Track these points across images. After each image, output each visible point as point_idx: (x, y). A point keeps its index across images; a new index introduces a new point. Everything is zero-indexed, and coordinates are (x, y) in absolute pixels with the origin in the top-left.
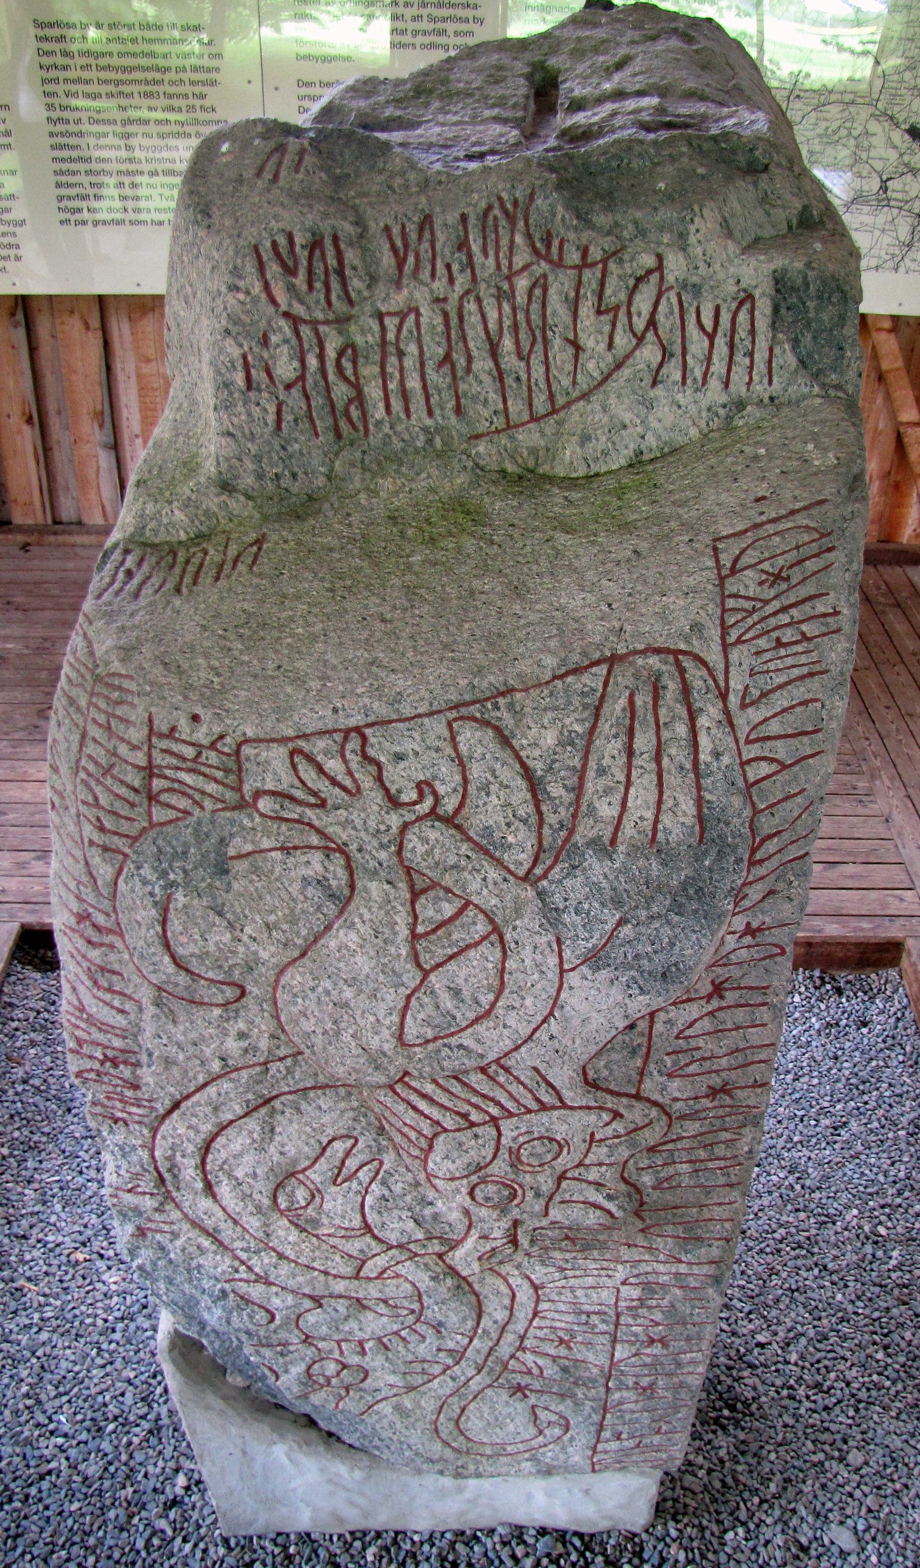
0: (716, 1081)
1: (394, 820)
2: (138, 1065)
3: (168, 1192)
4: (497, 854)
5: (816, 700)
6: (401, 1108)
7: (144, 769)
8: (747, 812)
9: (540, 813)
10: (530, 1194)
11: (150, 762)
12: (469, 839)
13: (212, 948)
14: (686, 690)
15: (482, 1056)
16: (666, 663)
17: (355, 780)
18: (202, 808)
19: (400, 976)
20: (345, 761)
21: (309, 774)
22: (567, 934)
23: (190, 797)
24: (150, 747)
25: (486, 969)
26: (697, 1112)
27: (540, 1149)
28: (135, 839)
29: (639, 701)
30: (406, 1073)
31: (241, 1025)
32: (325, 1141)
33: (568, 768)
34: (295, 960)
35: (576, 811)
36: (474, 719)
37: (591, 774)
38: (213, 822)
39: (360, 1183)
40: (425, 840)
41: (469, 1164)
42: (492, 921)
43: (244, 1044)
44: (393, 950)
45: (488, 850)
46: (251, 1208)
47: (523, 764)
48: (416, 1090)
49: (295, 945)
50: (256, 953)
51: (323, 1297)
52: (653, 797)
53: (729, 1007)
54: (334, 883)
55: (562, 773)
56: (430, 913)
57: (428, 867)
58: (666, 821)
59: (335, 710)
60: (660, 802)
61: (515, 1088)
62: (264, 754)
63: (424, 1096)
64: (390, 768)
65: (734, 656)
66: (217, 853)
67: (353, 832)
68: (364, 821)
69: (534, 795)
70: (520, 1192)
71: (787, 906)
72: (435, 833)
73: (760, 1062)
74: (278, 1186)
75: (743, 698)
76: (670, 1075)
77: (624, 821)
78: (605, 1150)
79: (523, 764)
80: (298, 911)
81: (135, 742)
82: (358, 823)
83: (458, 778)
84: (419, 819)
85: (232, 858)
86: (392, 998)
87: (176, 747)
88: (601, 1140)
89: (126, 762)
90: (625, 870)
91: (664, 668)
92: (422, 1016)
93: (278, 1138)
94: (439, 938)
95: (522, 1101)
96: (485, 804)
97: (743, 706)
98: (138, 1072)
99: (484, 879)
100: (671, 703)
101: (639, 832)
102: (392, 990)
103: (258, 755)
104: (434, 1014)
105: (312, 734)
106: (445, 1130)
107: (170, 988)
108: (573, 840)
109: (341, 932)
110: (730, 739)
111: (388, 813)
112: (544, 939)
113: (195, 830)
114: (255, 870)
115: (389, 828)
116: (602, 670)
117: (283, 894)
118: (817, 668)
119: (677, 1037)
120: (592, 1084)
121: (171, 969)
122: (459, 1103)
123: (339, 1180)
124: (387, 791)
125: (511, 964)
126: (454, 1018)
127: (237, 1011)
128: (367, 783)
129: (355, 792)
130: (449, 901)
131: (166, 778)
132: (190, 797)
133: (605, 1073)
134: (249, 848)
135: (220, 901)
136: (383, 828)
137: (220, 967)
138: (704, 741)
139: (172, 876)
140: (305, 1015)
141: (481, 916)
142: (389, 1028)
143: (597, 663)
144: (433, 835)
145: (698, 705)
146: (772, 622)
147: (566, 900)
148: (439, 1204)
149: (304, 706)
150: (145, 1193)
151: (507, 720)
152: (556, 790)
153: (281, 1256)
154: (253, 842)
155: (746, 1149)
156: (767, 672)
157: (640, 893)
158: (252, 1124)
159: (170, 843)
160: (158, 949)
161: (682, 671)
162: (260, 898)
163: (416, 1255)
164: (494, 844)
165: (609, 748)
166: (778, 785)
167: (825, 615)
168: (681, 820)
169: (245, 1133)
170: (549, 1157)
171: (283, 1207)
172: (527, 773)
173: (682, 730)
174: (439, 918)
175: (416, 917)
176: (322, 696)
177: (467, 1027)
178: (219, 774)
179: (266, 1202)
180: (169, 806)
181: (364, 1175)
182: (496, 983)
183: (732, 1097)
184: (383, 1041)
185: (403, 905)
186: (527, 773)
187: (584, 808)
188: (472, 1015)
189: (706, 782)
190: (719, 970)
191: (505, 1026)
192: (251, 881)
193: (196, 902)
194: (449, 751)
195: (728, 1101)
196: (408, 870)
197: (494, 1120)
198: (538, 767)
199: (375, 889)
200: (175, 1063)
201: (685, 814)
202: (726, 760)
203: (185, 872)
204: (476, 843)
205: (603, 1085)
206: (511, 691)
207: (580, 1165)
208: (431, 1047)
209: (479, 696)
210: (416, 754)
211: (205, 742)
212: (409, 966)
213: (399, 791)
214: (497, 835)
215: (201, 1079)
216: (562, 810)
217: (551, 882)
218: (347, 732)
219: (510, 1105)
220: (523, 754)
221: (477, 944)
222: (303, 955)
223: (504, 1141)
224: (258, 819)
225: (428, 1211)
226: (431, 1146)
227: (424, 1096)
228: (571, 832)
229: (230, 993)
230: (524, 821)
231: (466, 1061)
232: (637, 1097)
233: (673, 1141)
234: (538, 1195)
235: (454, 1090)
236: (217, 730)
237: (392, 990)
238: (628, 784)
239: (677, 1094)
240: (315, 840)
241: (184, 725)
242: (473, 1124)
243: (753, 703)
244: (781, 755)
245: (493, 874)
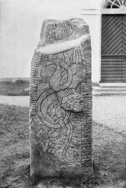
0: (87, 93)
165: (74, 54)
170: (73, 101)
181: (56, 107)
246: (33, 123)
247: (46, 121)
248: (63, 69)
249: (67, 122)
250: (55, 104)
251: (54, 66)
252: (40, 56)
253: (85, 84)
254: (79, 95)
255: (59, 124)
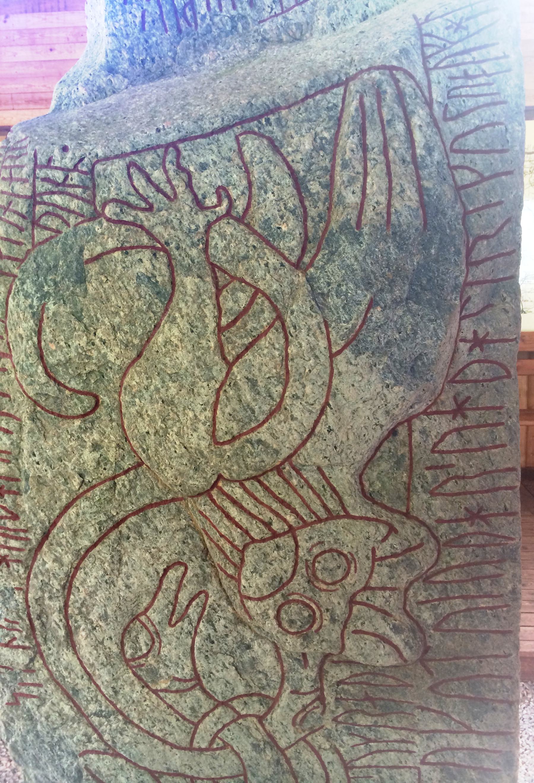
0: (472, 502)
1: (201, 220)
2: (18, 493)
3: (38, 645)
4: (275, 244)
5: (501, 124)
6: (217, 516)
7: (31, 197)
8: (458, 208)
9: (304, 208)
10: (327, 616)
11: (34, 192)
12: (255, 232)
13: (73, 354)
14: (400, 96)
15: (277, 452)
16: (384, 74)
17: (173, 188)
18: (68, 225)
19: (210, 369)
20: (166, 172)
21: (140, 182)
22: (332, 318)
23: (60, 217)
24: (35, 177)
25: (274, 357)
26: (461, 537)
27: (332, 565)
28: (22, 261)
29: (367, 101)
30: (220, 477)
31: (96, 436)
32: (161, 568)
33: (322, 169)
34: (134, 361)
35: (330, 204)
36: (254, 133)
37: (338, 168)
38: (75, 234)
39: (190, 623)
40: (223, 236)
41: (274, 579)
42: (275, 308)
43: (97, 455)
44: (204, 342)
45: (268, 239)
46: (103, 658)
47: (290, 167)
48: (229, 497)
49: (134, 345)
50: (105, 356)
51: (162, 774)
52: (384, 186)
53: (472, 427)
54: (159, 279)
55: (318, 173)
56: (230, 304)
57: (227, 261)
58: (397, 205)
59: (158, 130)
60: (390, 189)
61: (305, 492)
62: (109, 168)
63: (235, 502)
64: (196, 175)
65: (434, 75)
66: (77, 260)
67: (172, 231)
68: (178, 222)
69: (299, 193)
70: (318, 614)
71: (503, 316)
72: (228, 228)
73: (507, 488)
74: (125, 630)
75: (445, 113)
76: (433, 494)
77: (365, 207)
78: (386, 570)
79: (290, 167)
80: (135, 310)
81: (24, 177)
82: (176, 222)
83: (245, 182)
84: (219, 219)
85: (88, 261)
86: (205, 392)
87: (50, 173)
88: (382, 559)
89: (18, 196)
90: (369, 253)
91: (383, 78)
92: (228, 410)
93: (124, 569)
94: (238, 329)
95: (313, 507)
96: (264, 200)
97: (445, 119)
98: (19, 500)
99: (267, 265)
100: (391, 104)
101: (377, 214)
102: (205, 384)
103: (105, 170)
104: (237, 407)
105: (143, 150)
106: (253, 541)
107: (42, 401)
108: (330, 228)
109: (166, 326)
110: (438, 138)
111: (196, 213)
112: (314, 321)
113: (64, 244)
114: (104, 272)
115: (198, 227)
116: (341, 90)
117: (125, 295)
118: (497, 98)
119: (433, 451)
120: (368, 497)
121: (43, 379)
122: (263, 509)
123: (174, 620)
124: (195, 196)
125: (292, 350)
126: (253, 412)
127: (93, 422)
128: (181, 189)
129: (173, 198)
130: (243, 291)
131: (45, 203)
132: (60, 217)
133: (378, 485)
134: (99, 250)
135: (79, 307)
136: (193, 227)
137: (80, 375)
138: (418, 136)
139: (46, 288)
140: (141, 416)
141: (267, 303)
142: (204, 424)
143: (338, 85)
144: (229, 230)
145: (410, 108)
146: (460, 59)
147: (329, 284)
148: (256, 647)
149: (138, 130)
150: (18, 647)
151: (278, 134)
152: (314, 187)
153: (128, 720)
154: (101, 244)
155: (510, 587)
156: (461, 96)
157: (383, 275)
158: (103, 551)
159: (45, 258)
160: (34, 359)
161: (397, 81)
162: (108, 300)
163: (240, 716)
164: (271, 235)
165: (349, 143)
166: (481, 192)
167: (497, 58)
168: (408, 203)
169: (98, 563)
170: (340, 573)
171: (128, 656)
172: (293, 174)
173: (400, 127)
174: (236, 308)
175: (220, 310)
176: (148, 125)
177: (264, 422)
178: (79, 191)
179: (115, 649)
180: (46, 228)
182: (283, 372)
183: (488, 524)
184: (199, 439)
185: (210, 298)
186: (293, 174)
187: (335, 199)
188: (266, 408)
189: (424, 173)
190: (460, 387)
191: (293, 418)
192: (101, 283)
193: (62, 309)
194: (237, 160)
195: (486, 528)
196: (213, 266)
197: (291, 530)
198: (300, 167)
199: (189, 283)
200: (44, 484)
201: (410, 199)
202: (437, 156)
203: (56, 283)
204: (260, 235)
205: (377, 498)
206: (278, 108)
207: (367, 588)
208: (237, 444)
209: (256, 113)
210: (215, 163)
211: (70, 165)
212: (216, 358)
213: (204, 197)
214: (274, 226)
215: (65, 498)
216: (320, 204)
217: (317, 268)
218: (167, 146)
219: (303, 511)
220: (289, 159)
221: (265, 333)
222: (139, 356)
223: (301, 553)
224: (105, 224)
225: (247, 656)
226: (242, 560)
227: (235, 502)
228: (328, 223)
229: (88, 402)
230: (293, 212)
231: (264, 457)
232: (407, 515)
233: (444, 571)
234: (333, 620)
235: (257, 495)
236: (78, 154)
237: (205, 384)
238: (366, 174)
239: (440, 514)
240: (145, 240)
241: (57, 153)
242: (275, 535)
243: (453, 119)
244: (479, 167)
245: (273, 260)
246: (19, 726)
247: (117, 723)
248: (236, 300)
249: (292, 735)
250: (184, 597)
251: (145, 263)
252: (25, 172)
253: (459, 422)
254: (395, 520)
255: (226, 745)
